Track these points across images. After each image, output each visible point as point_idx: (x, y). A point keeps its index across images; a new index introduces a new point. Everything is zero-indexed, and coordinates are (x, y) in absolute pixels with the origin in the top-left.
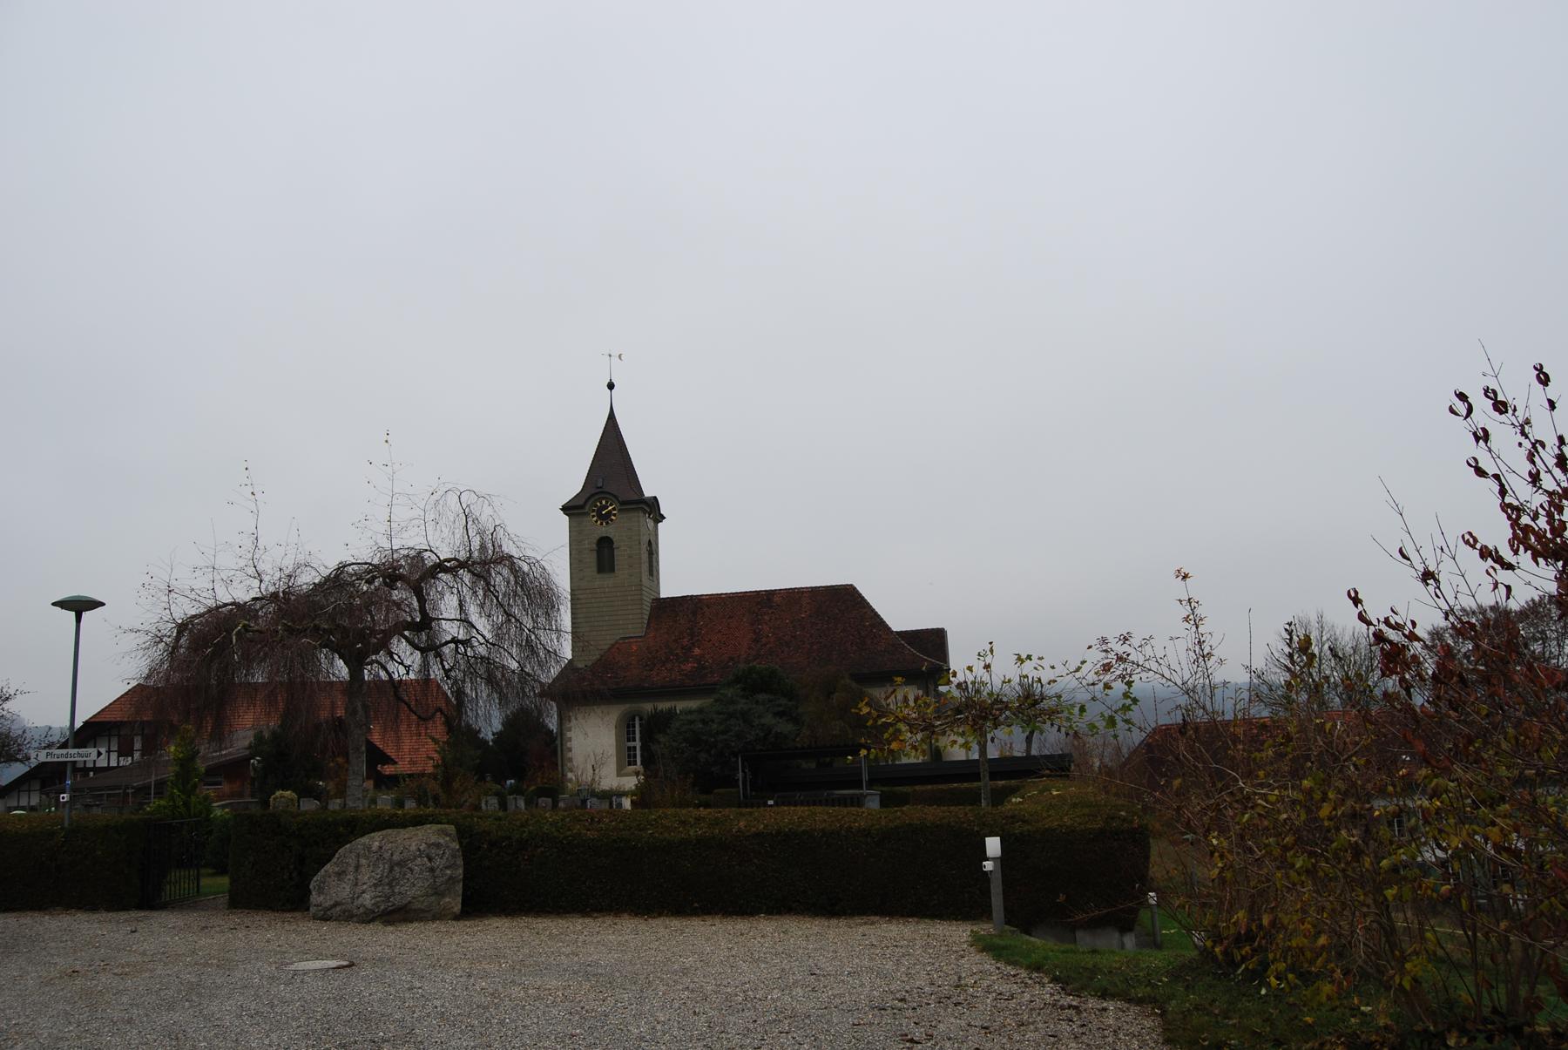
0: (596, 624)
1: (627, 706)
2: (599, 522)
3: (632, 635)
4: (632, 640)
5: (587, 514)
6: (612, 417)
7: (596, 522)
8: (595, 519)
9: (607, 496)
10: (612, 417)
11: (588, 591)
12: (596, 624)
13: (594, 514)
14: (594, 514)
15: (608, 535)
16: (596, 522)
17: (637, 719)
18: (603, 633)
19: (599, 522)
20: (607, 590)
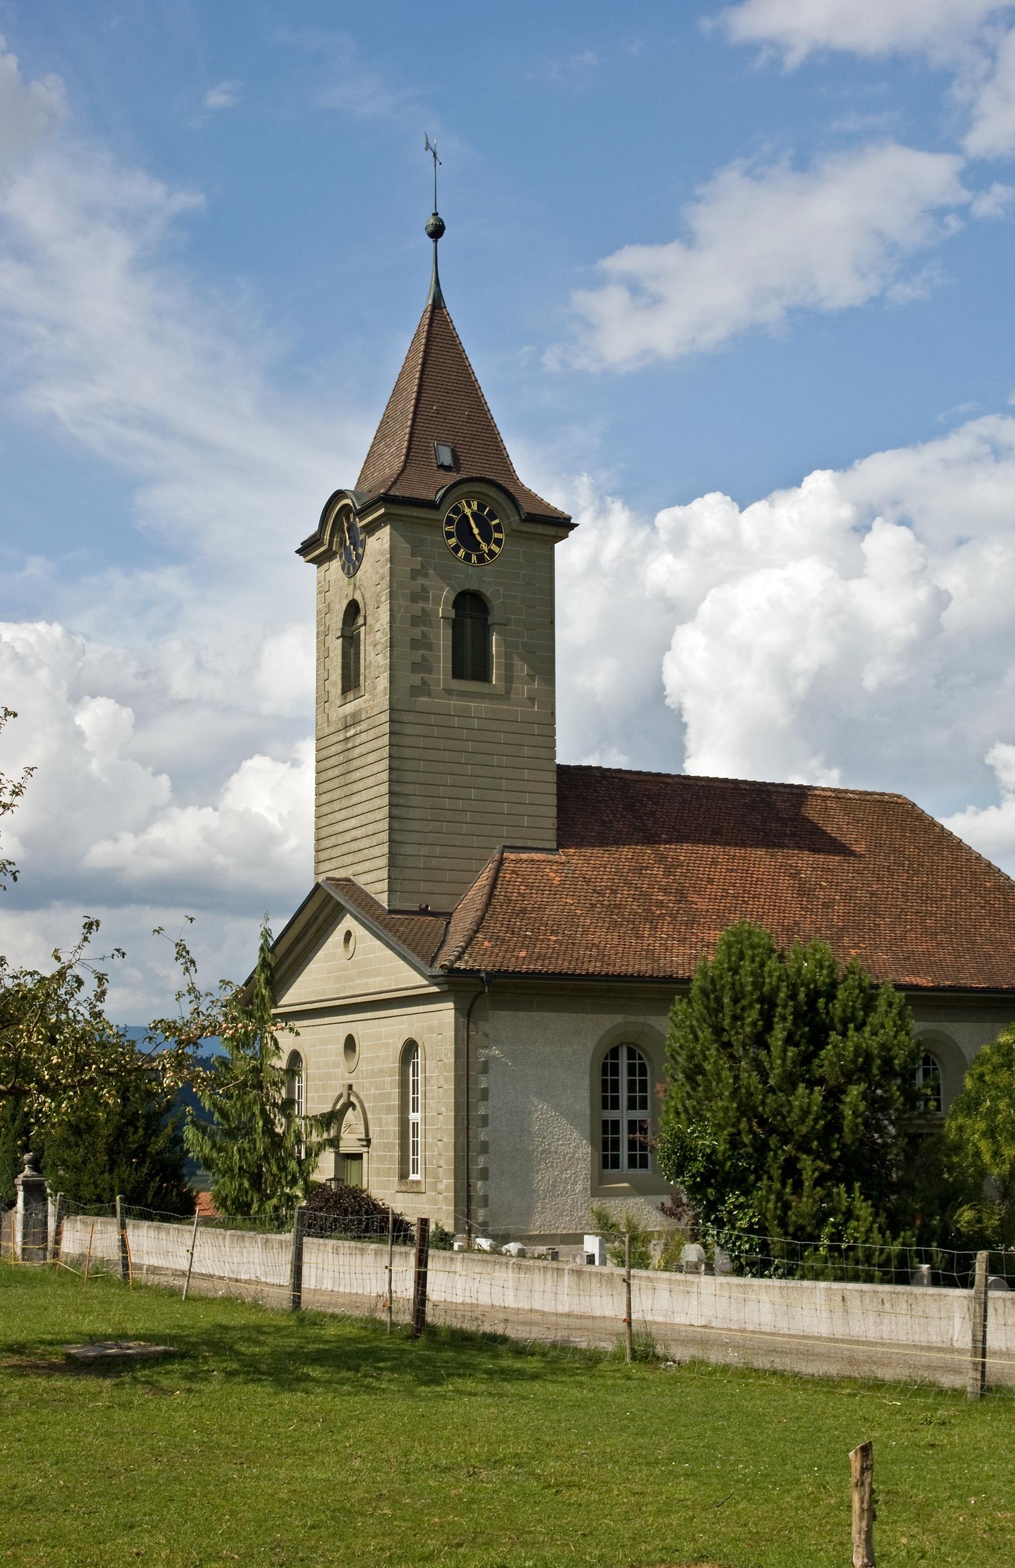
0: (447, 803)
1: (619, 1018)
2: (462, 553)
3: (530, 844)
4: (536, 856)
5: (435, 524)
6: (438, 304)
7: (456, 549)
8: (453, 541)
9: (493, 492)
10: (438, 304)
11: (432, 719)
12: (447, 803)
13: (451, 529)
14: (451, 529)
15: (483, 589)
16: (456, 549)
17: (623, 1053)
18: (465, 828)
19: (462, 553)
20: (476, 723)
